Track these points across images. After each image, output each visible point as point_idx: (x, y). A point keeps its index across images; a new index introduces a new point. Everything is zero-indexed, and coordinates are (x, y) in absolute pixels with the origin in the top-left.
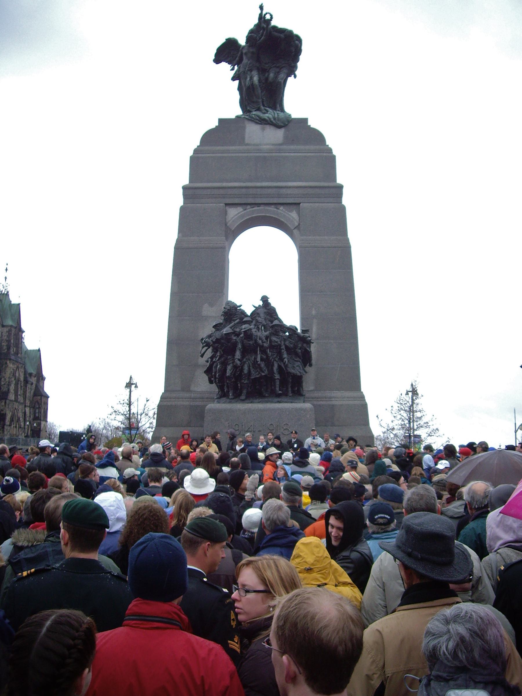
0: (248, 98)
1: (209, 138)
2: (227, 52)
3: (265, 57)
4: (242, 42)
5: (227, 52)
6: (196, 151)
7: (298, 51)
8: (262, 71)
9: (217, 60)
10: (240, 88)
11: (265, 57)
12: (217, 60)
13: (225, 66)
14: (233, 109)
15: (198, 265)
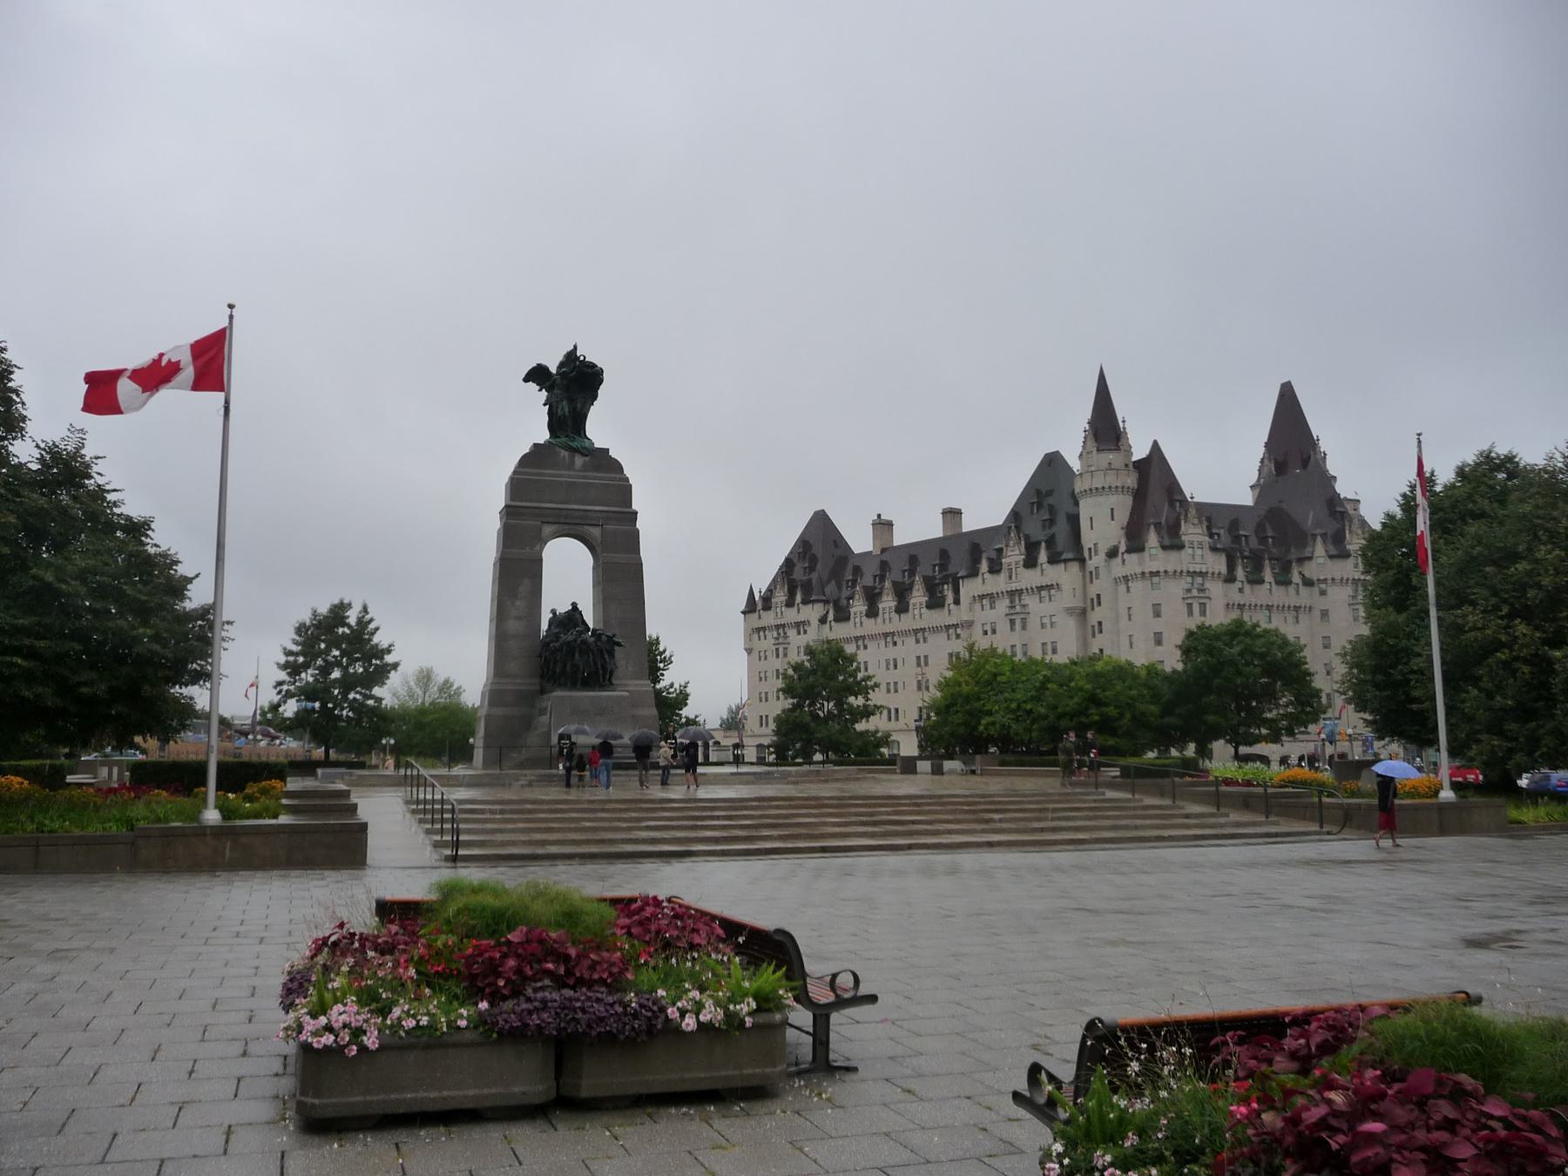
0: (555, 424)
1: (525, 461)
2: (538, 375)
3: (571, 386)
4: (553, 370)
5: (538, 375)
6: (515, 472)
7: (601, 381)
8: (571, 401)
9: (526, 380)
10: (550, 413)
11: (571, 386)
12: (526, 380)
13: (533, 386)
14: (543, 436)
15: (517, 572)
